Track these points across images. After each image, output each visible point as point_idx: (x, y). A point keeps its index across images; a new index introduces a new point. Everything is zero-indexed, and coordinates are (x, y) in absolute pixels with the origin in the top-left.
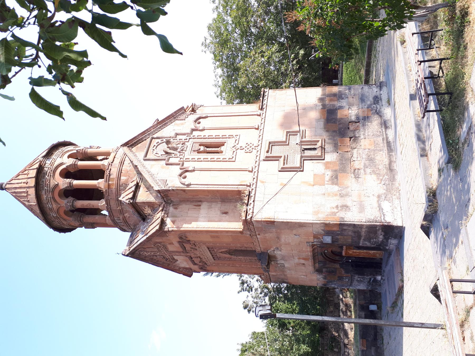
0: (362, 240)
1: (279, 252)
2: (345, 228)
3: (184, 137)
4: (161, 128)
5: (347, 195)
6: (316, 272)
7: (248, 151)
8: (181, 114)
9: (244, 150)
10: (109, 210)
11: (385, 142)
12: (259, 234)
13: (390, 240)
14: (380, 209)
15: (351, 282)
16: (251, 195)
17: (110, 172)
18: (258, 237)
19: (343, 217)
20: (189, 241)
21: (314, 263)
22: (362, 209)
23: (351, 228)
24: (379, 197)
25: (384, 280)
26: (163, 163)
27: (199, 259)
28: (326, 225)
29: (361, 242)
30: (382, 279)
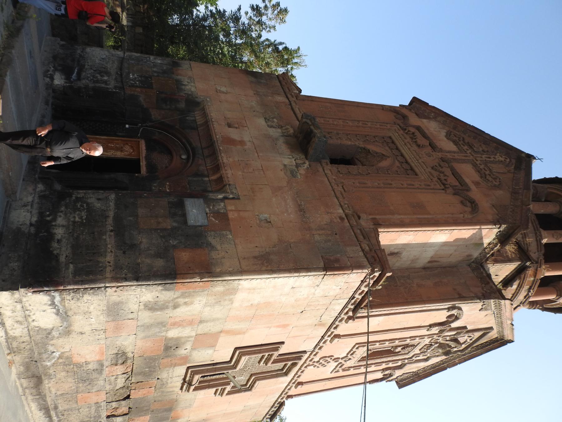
0: (111, 214)
1: (286, 161)
2: (160, 263)
3: (418, 358)
4: (442, 362)
5: (148, 327)
6: (199, 100)
7: (329, 359)
8: (405, 379)
9: (333, 358)
10: (538, 233)
11: (51, 407)
12: (342, 219)
13: (34, 219)
14: (64, 315)
15: (121, 69)
16: (352, 307)
17: (528, 294)
18: (341, 211)
19: (163, 292)
20: (455, 194)
21: (207, 124)
22: (114, 311)
23: (145, 261)
24: (67, 332)
25: (45, 74)
26: (469, 328)
27: (419, 142)
28: (207, 270)
29: (112, 204)
30: (52, 78)
